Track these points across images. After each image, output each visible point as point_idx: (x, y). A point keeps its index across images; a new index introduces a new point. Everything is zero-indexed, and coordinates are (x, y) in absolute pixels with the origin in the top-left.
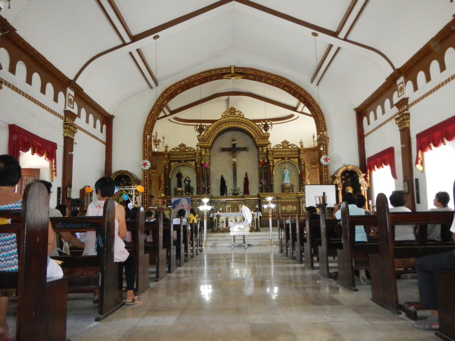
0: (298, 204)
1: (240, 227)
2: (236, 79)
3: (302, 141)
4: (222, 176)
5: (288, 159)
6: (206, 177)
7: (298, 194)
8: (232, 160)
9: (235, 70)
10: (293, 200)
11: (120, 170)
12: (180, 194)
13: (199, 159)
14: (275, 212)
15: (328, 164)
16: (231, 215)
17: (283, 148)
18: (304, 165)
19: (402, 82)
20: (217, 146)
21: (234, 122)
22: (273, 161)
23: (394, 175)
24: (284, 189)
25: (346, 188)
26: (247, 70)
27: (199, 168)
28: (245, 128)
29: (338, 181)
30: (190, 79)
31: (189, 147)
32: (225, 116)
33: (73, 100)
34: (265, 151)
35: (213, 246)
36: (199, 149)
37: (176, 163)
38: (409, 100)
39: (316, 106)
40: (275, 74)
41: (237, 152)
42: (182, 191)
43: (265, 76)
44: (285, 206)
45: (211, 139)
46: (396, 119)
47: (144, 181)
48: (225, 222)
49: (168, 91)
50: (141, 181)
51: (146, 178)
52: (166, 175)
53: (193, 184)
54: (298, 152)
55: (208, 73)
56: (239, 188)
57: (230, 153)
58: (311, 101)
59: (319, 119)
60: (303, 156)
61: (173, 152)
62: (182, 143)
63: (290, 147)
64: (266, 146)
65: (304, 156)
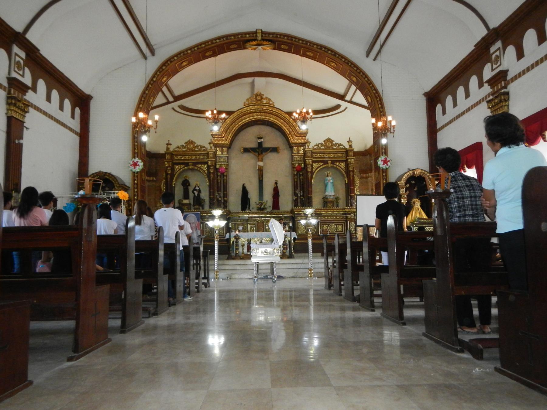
0: (344, 223)
1: (266, 250)
2: (264, 49)
3: (351, 140)
4: (244, 185)
5: (331, 163)
7: (344, 209)
8: (257, 163)
9: (262, 36)
10: (338, 217)
11: (99, 171)
12: (187, 208)
13: (213, 161)
14: (314, 233)
15: (387, 167)
16: (255, 236)
17: (325, 149)
18: (353, 171)
19: (499, 49)
21: (260, 112)
22: (312, 165)
24: (326, 202)
25: (412, 201)
26: (279, 36)
27: (213, 173)
28: (276, 121)
30: (200, 47)
31: (200, 145)
32: (249, 104)
33: (24, 65)
34: (301, 152)
35: (227, 279)
36: (213, 148)
37: (182, 166)
38: (509, 73)
39: (373, 88)
40: (317, 43)
41: (264, 153)
42: (190, 204)
43: (304, 45)
44: (327, 226)
45: (230, 136)
46: (488, 102)
47: (134, 187)
48: (246, 246)
49: (169, 63)
50: (129, 188)
51: (137, 184)
52: (168, 182)
53: (205, 195)
54: (345, 154)
55: (225, 39)
56: (267, 201)
57: (255, 155)
58: (367, 81)
59: (377, 105)
60: (351, 161)
61: (178, 151)
62: (189, 140)
63: (335, 147)
64: (303, 146)
65: (353, 159)
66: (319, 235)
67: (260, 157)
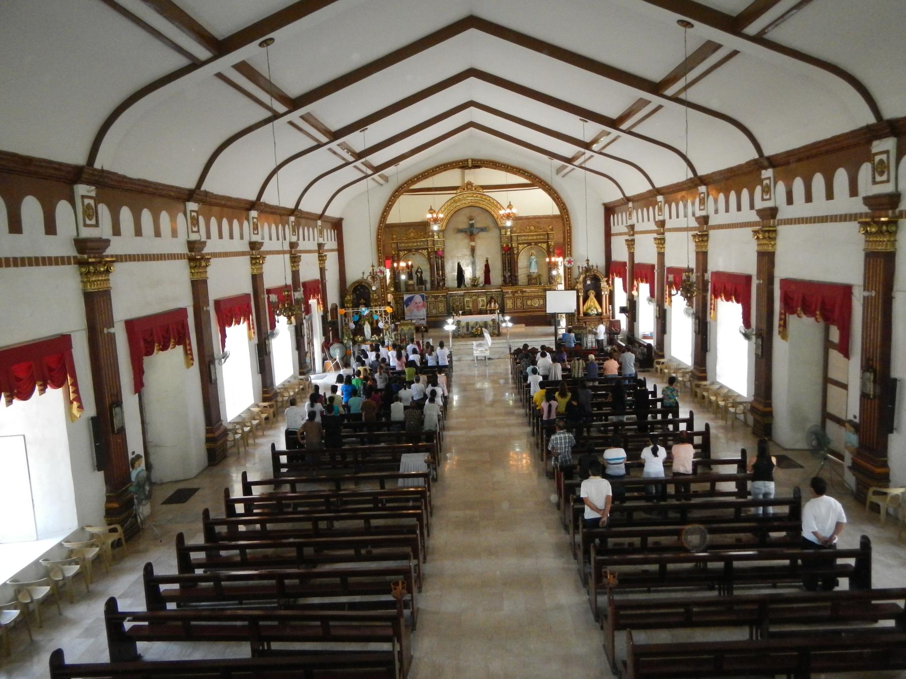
22: (518, 248)
23: (625, 289)
29: (580, 286)
34: (509, 233)
37: (406, 252)
53: (426, 276)
66: (524, 309)
67: (472, 237)
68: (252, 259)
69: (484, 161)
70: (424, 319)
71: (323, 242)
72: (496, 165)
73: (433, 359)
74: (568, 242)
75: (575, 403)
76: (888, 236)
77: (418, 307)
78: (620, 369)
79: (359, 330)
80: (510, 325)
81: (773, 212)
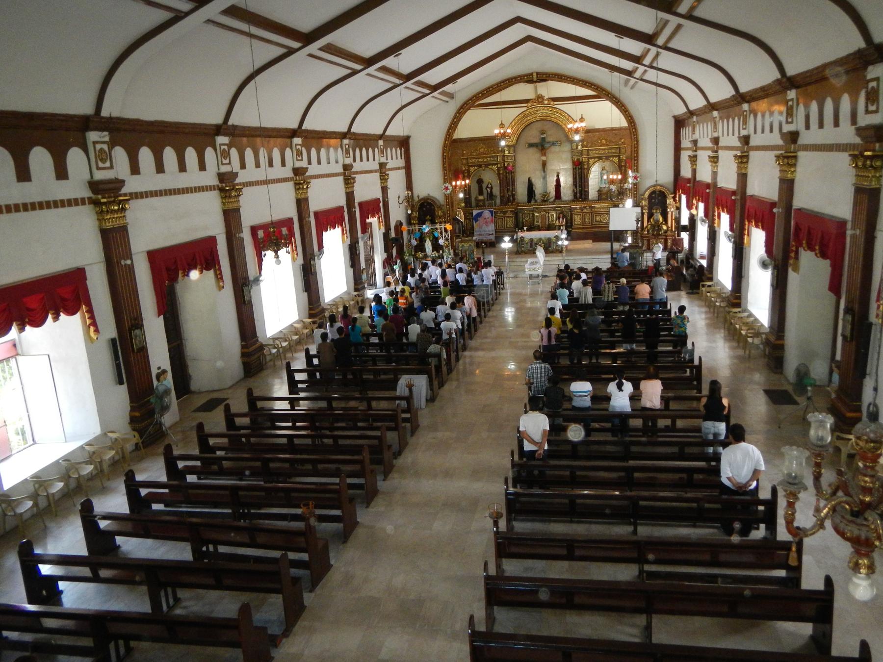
4: (529, 179)
6: (511, 182)
9: (537, 77)
20: (523, 141)
22: (588, 162)
29: (645, 203)
53: (496, 191)
56: (550, 193)
66: (592, 225)
68: (296, 184)
69: (549, 74)
70: (492, 234)
71: (386, 162)
72: (561, 78)
73: (478, 278)
74: (635, 157)
75: (576, 331)
76: (873, 171)
77: (486, 222)
78: (652, 292)
79: (421, 247)
80: (566, 243)
81: (793, 137)
